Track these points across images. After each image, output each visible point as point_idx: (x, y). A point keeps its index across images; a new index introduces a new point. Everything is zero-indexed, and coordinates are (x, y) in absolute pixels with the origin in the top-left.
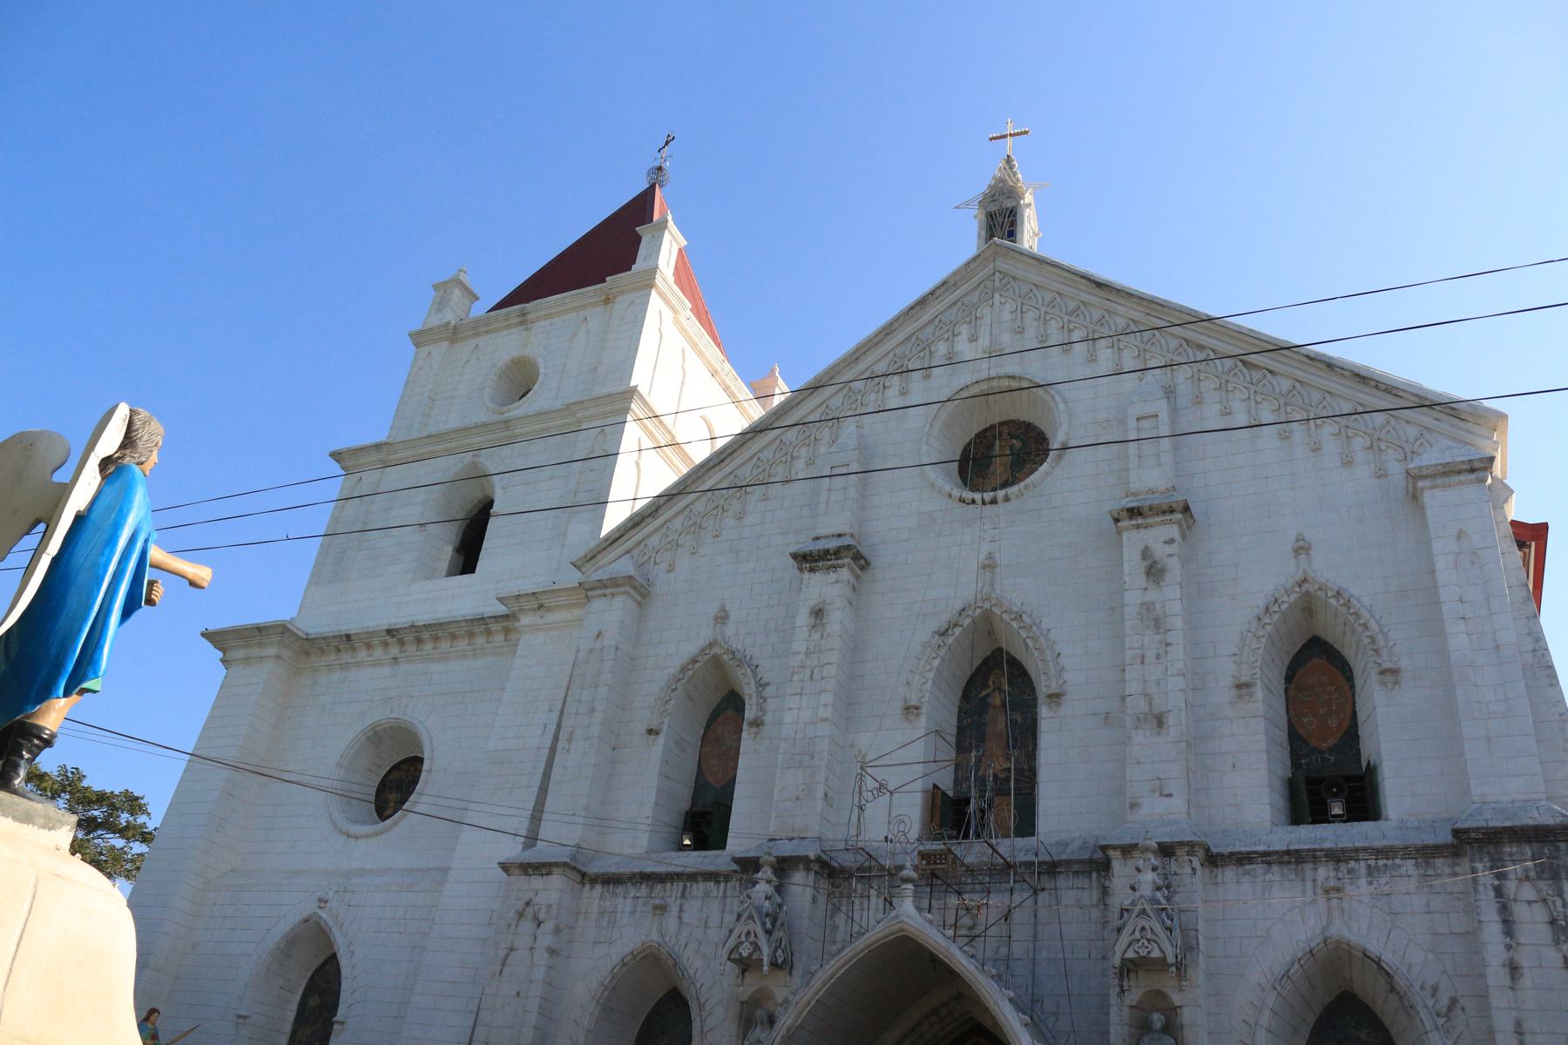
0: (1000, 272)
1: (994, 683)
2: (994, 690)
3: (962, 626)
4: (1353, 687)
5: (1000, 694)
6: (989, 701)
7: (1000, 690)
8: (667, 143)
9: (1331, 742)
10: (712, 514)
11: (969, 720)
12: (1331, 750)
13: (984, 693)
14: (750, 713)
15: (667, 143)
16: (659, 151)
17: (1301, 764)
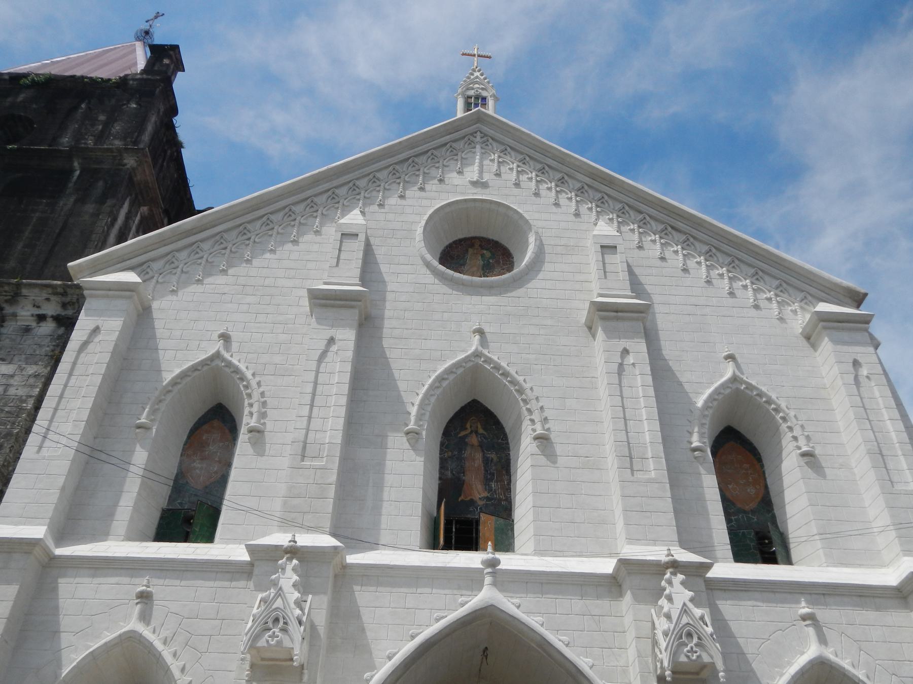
0: (481, 133)
1: (471, 427)
2: (471, 432)
3: (456, 374)
4: (762, 466)
5: (477, 436)
6: (467, 440)
7: (476, 432)
8: (156, 17)
9: (752, 505)
10: (220, 253)
11: (450, 454)
12: (753, 512)
13: (463, 434)
14: (247, 421)
15: (156, 17)
16: (147, 22)
17: (732, 519)
